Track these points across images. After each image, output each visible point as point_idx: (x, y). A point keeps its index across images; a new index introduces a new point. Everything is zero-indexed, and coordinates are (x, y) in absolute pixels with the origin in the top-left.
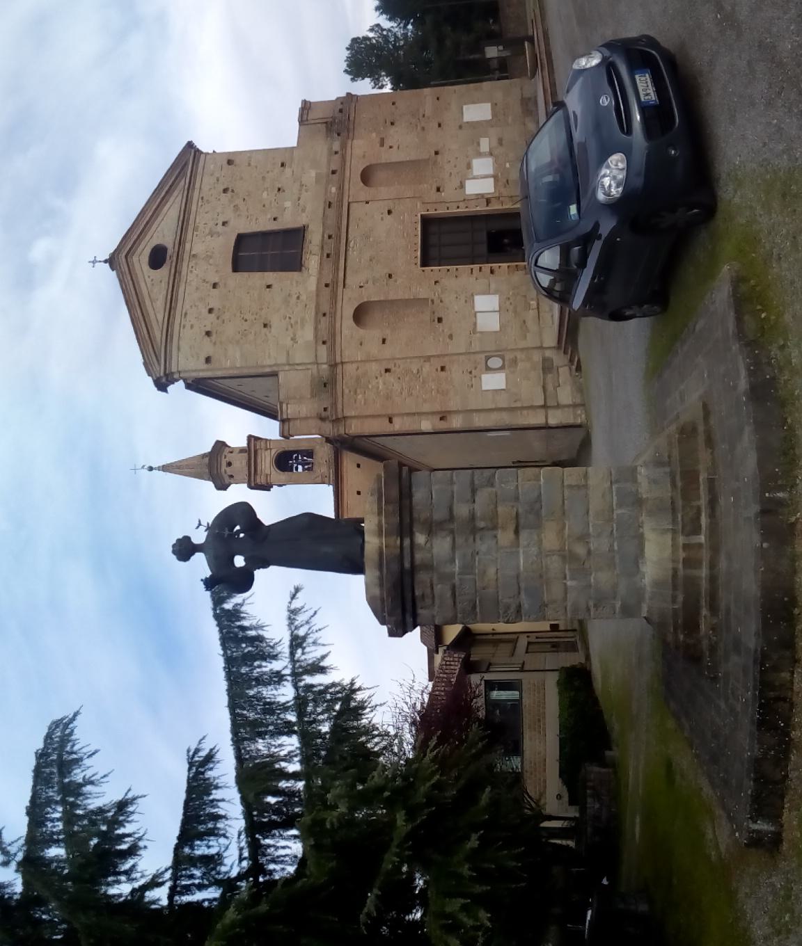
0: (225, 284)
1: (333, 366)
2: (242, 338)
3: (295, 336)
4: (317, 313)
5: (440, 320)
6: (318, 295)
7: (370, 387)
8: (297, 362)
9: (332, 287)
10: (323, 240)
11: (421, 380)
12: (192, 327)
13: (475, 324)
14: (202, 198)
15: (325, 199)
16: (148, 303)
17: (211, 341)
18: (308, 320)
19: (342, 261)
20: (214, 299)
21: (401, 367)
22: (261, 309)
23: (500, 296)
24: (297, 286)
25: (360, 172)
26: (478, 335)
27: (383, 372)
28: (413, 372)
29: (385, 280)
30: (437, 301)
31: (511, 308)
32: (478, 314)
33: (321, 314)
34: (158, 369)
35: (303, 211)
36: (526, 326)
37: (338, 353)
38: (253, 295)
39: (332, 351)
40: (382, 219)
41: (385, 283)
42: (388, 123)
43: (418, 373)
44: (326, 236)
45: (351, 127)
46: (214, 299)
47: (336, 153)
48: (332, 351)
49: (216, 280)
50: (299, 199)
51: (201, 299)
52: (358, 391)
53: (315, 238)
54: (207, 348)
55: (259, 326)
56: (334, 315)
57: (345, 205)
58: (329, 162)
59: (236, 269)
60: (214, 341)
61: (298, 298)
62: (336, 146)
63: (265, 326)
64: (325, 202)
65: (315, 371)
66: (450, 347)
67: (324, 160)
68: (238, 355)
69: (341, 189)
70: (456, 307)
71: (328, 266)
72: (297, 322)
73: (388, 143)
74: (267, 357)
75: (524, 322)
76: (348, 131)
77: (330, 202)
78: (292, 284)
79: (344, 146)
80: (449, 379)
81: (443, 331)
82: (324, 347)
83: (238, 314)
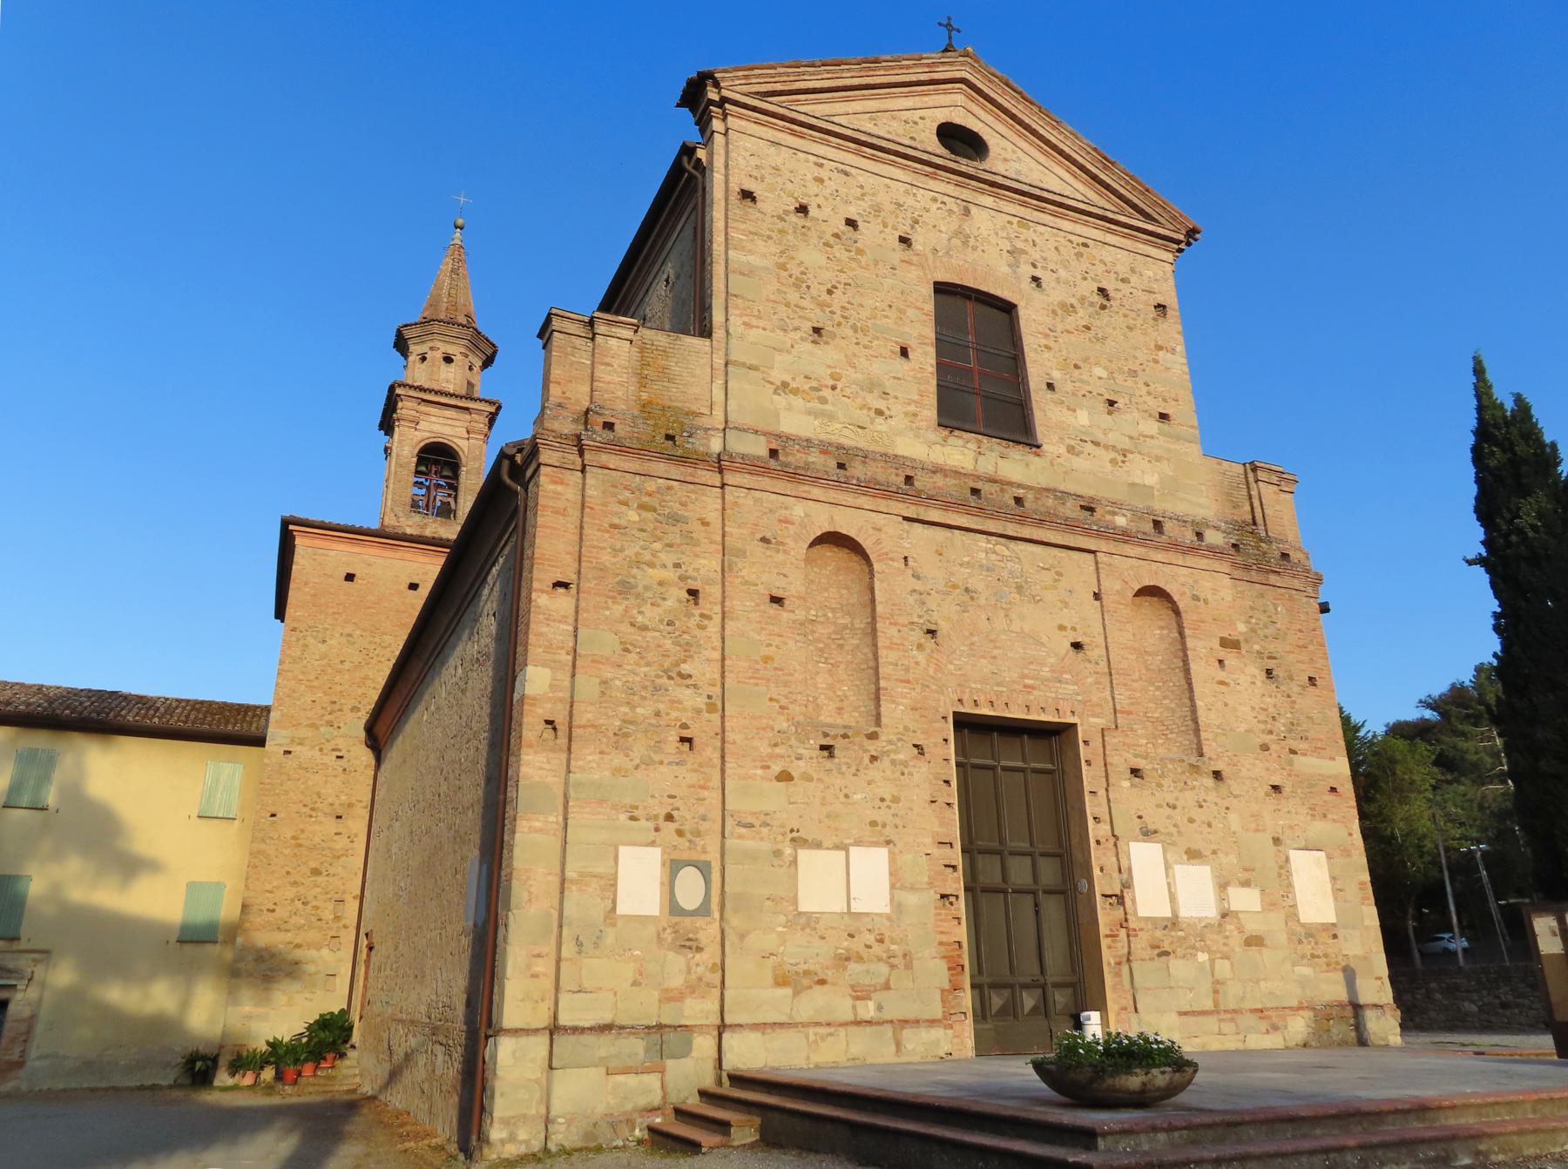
0: (909, 263)
1: (720, 464)
2: (791, 276)
3: (795, 392)
7: (657, 546)
10: (1010, 484)
11: (658, 681)
12: (820, 180)
13: (818, 845)
17: (786, 212)
18: (829, 429)
21: (697, 632)
23: (889, 918)
24: (906, 414)
25: (1161, 585)
26: (788, 851)
27: (693, 585)
28: (684, 662)
29: (922, 621)
30: (872, 748)
31: (857, 945)
32: (843, 853)
34: (738, 88)
36: (811, 987)
37: (746, 480)
38: (887, 317)
39: (753, 466)
40: (1062, 628)
41: (916, 620)
43: (680, 675)
44: (1020, 492)
45: (1254, 576)
47: (1199, 535)
48: (753, 466)
49: (917, 246)
50: (1097, 444)
52: (650, 515)
54: (773, 202)
55: (819, 318)
56: (840, 484)
57: (1090, 543)
60: (786, 217)
61: (879, 412)
62: (1213, 538)
63: (817, 330)
66: (759, 772)
67: (1181, 508)
68: (753, 259)
69: (1125, 536)
70: (857, 797)
72: (823, 401)
73: (1231, 659)
74: (746, 319)
75: (822, 982)
78: (909, 404)
79: (1214, 552)
80: (657, 758)
81: (799, 758)
82: (763, 452)
83: (843, 278)
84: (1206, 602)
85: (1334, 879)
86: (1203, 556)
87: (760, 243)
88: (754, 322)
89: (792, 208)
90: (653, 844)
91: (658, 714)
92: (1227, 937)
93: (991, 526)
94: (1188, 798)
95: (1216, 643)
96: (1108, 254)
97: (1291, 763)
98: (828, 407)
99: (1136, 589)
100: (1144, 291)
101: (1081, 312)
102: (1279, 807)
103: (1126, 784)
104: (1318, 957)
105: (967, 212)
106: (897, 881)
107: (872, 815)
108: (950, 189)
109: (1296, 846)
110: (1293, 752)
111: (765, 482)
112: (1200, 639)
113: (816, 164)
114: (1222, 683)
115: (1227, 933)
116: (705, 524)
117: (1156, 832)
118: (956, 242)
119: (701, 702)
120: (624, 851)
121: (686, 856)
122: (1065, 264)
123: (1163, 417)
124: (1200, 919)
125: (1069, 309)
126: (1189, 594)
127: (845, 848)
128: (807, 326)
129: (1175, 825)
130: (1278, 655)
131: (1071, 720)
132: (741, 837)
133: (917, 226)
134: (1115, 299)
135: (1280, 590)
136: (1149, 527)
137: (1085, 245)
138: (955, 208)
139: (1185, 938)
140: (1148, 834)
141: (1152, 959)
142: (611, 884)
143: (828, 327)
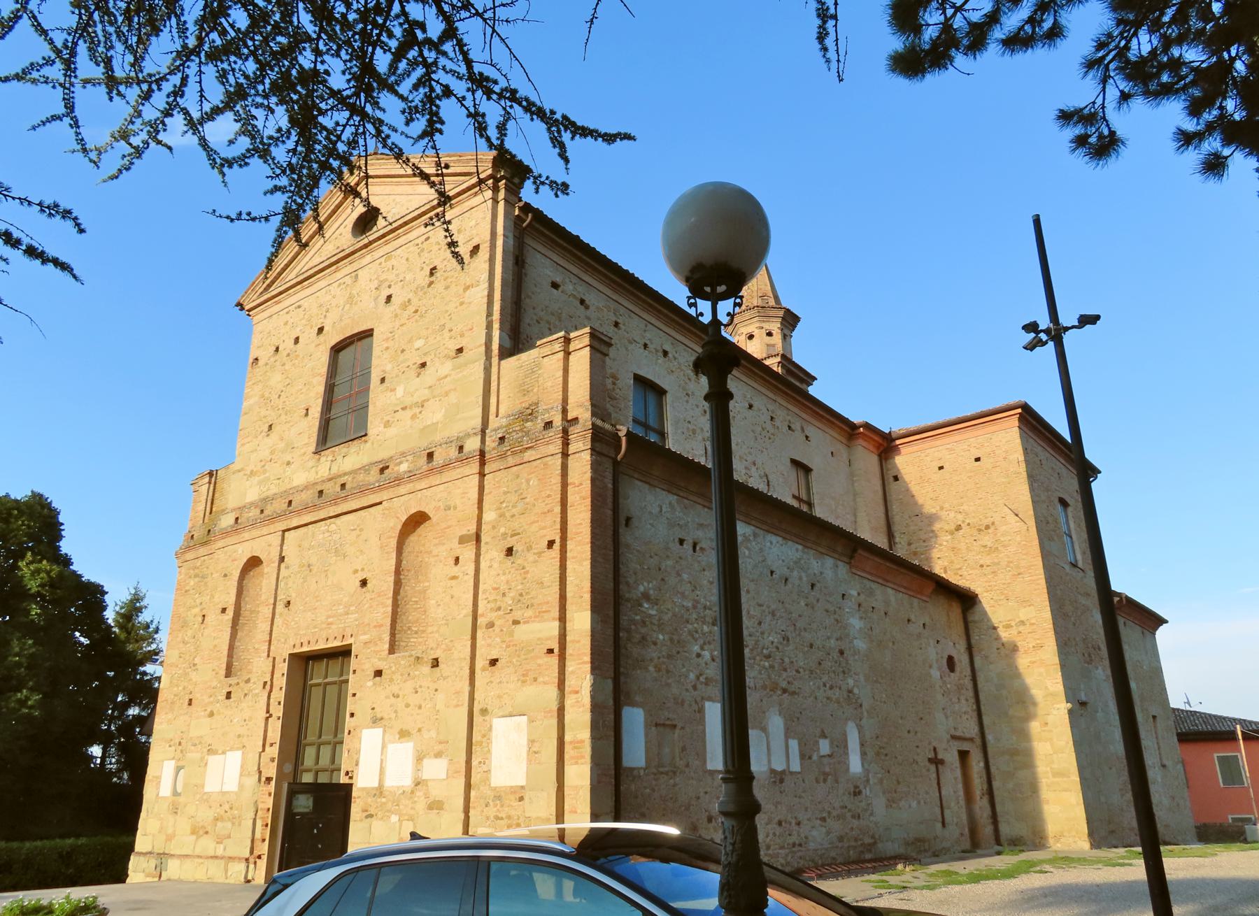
14: (428, 239)
23: (236, 793)
42: (510, 542)
45: (511, 460)
47: (461, 448)
70: (235, 720)
85: (532, 742)
86: (454, 467)
92: (415, 802)
94: (409, 686)
97: (511, 634)
99: (404, 520)
102: (492, 679)
103: (370, 684)
104: (502, 819)
109: (501, 714)
110: (516, 622)
112: (444, 544)
113: (287, 313)
114: (454, 578)
115: (416, 799)
117: (382, 719)
118: (347, 307)
123: (460, 350)
124: (398, 788)
130: (520, 531)
135: (534, 463)
139: (385, 803)
140: (376, 721)
141: (361, 820)
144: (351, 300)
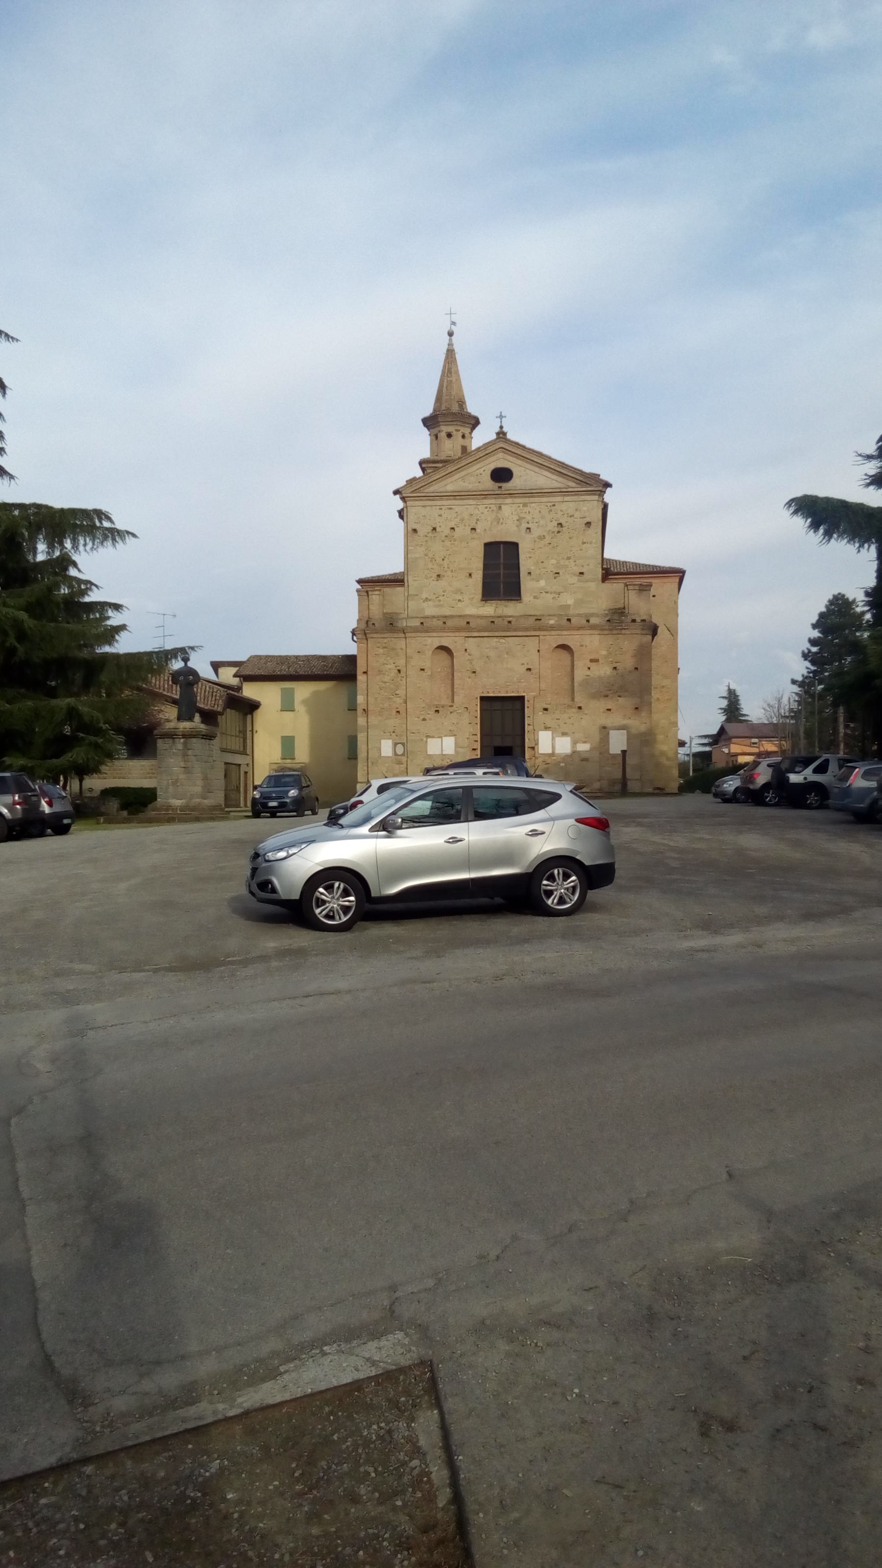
3: (430, 600)
4: (446, 617)
5: (437, 711)
6: (460, 616)
7: (388, 658)
8: (409, 603)
9: (467, 626)
12: (440, 516)
13: (433, 737)
15: (543, 616)
16: (463, 473)
17: (428, 533)
19: (486, 634)
20: (462, 531)
21: (400, 682)
22: (452, 571)
23: (453, 755)
25: (566, 643)
26: (425, 739)
27: (398, 668)
30: (451, 709)
32: (440, 739)
33: (445, 620)
35: (535, 597)
37: (413, 635)
39: (416, 630)
40: (523, 664)
43: (396, 694)
45: (615, 632)
46: (462, 531)
47: (588, 621)
49: (478, 531)
50: (547, 592)
51: (462, 520)
53: (510, 609)
58: (579, 615)
59: (488, 545)
61: (459, 600)
62: (593, 621)
63: (439, 576)
64: (540, 616)
65: (403, 616)
67: (582, 611)
68: (417, 555)
69: (552, 628)
70: (446, 724)
71: (483, 623)
72: (440, 601)
76: (610, 630)
77: (540, 620)
79: (594, 627)
81: (429, 714)
82: (418, 624)
83: (449, 552)
84: (586, 646)
87: (418, 548)
88: (416, 579)
89: (430, 531)
90: (390, 739)
91: (390, 705)
93: (497, 634)
95: (588, 661)
96: (564, 506)
98: (442, 603)
100: (580, 518)
101: (547, 537)
105: (500, 508)
106: (457, 746)
107: (451, 728)
108: (493, 501)
111: (419, 634)
116: (402, 649)
118: (495, 523)
119: (401, 701)
120: (383, 741)
121: (398, 742)
122: (543, 517)
123: (582, 573)
125: (541, 538)
126: (579, 644)
127: (441, 737)
128: (435, 575)
129: (559, 725)
131: (523, 694)
132: (412, 736)
133: (478, 522)
134: (565, 526)
136: (564, 622)
137: (554, 505)
138: (495, 509)
140: (546, 728)
142: (380, 749)
143: (442, 573)
144: (498, 520)
